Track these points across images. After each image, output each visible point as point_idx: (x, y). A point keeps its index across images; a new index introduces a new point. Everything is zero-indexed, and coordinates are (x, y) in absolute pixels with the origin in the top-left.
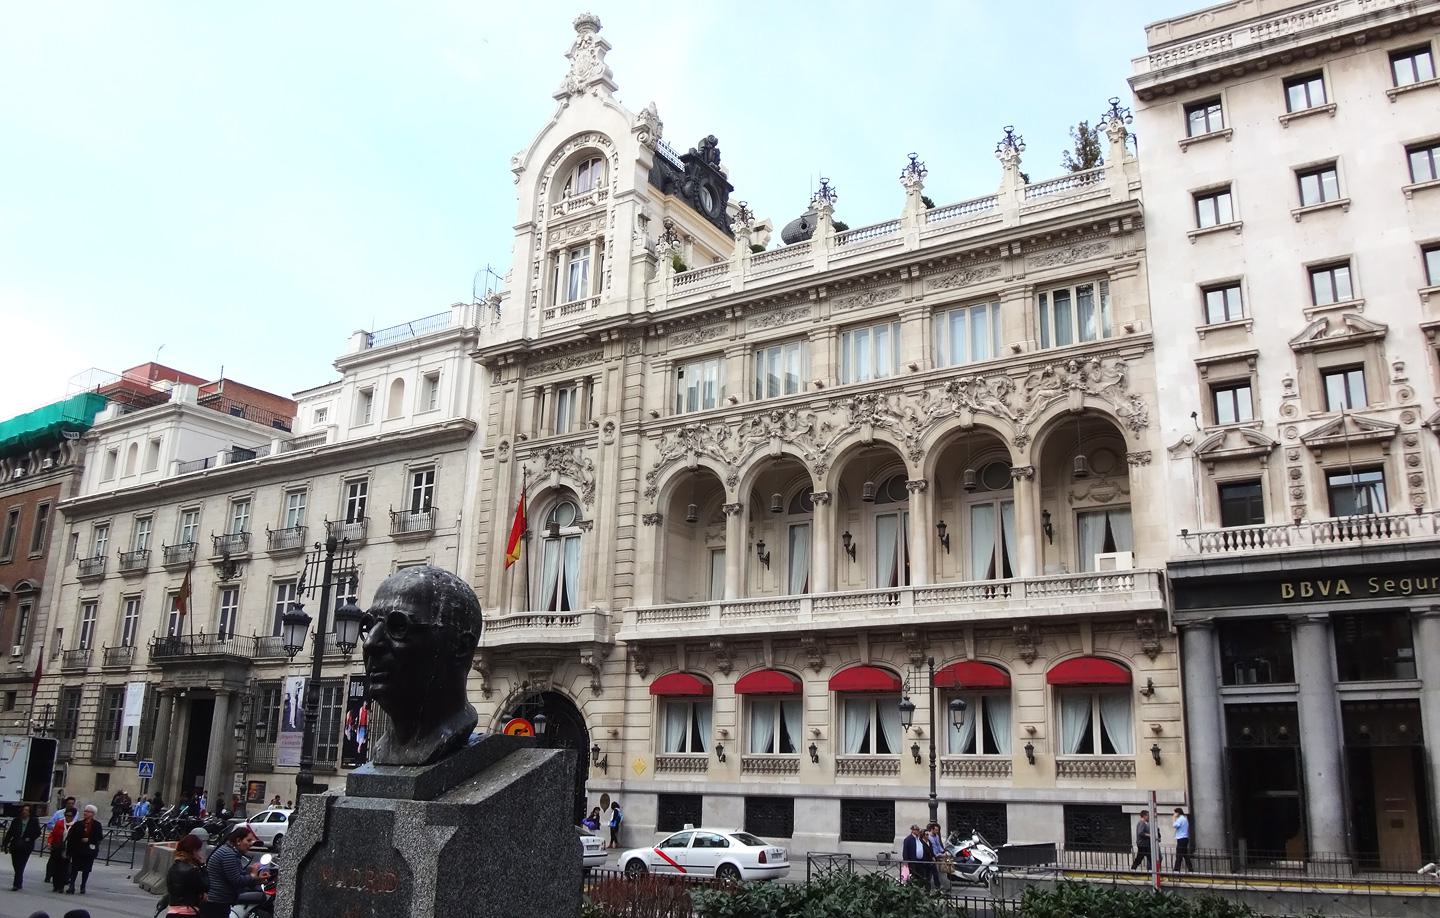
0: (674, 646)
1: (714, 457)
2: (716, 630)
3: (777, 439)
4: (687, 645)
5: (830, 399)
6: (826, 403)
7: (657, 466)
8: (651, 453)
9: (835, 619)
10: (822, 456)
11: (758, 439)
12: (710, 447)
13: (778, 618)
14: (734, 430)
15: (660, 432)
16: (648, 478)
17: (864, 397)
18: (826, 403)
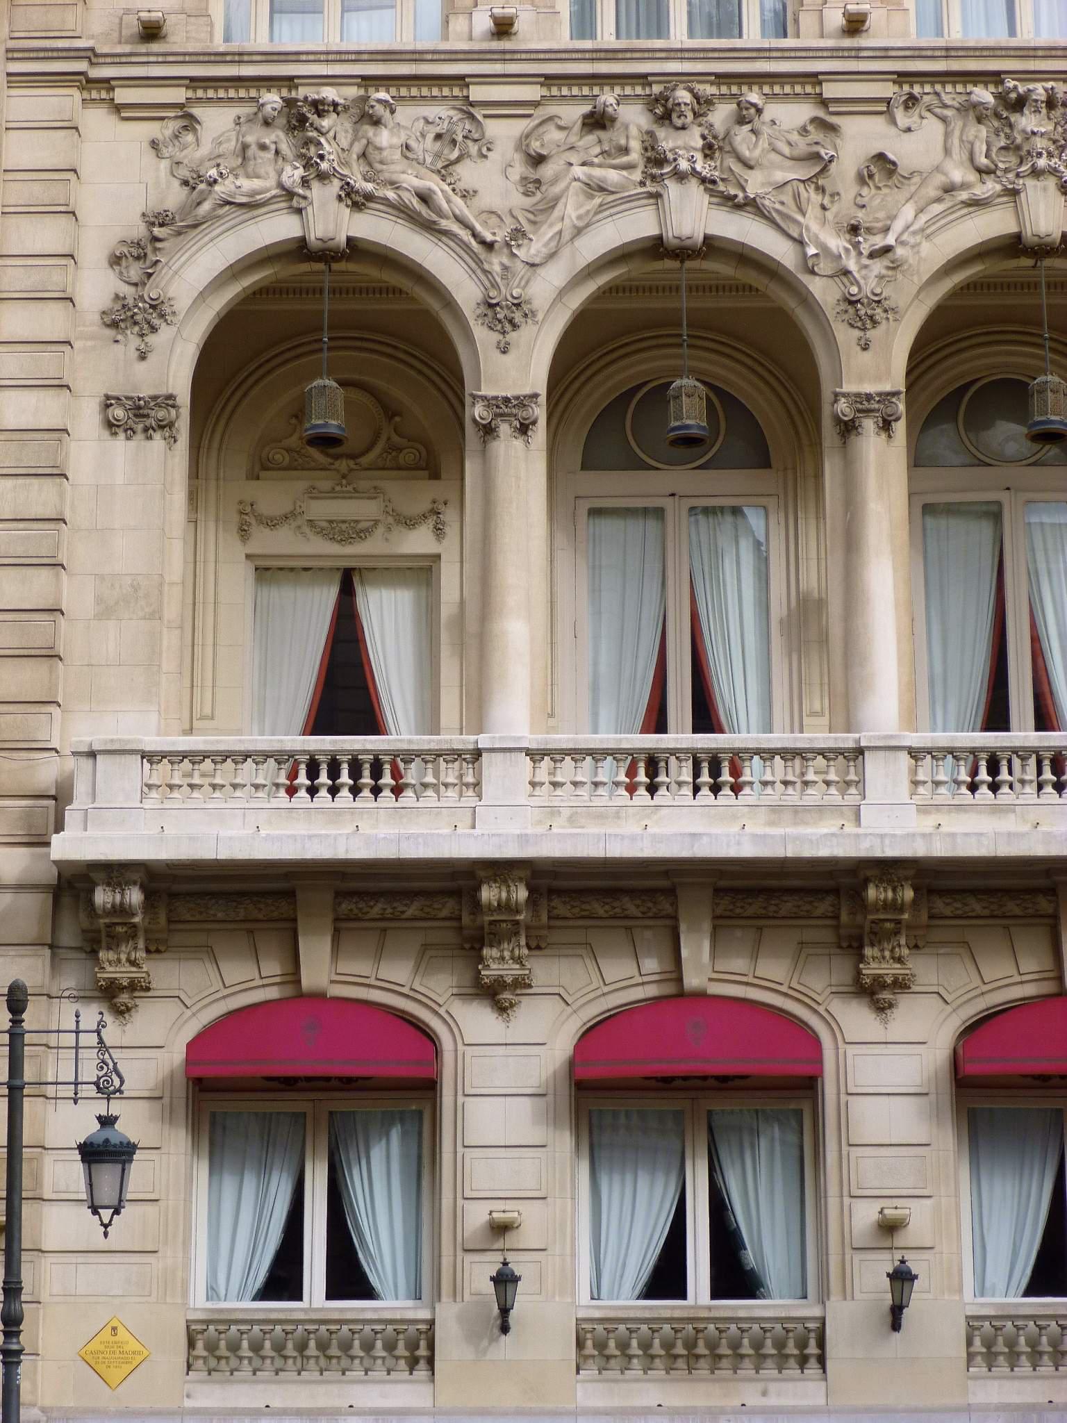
0: (290, 895)
1: (422, 215)
2: (523, 839)
3: (694, 187)
4: (340, 895)
5: (902, 77)
6: (886, 89)
7: (160, 219)
8: (121, 172)
9: (1009, 824)
10: (878, 266)
11: (613, 176)
12: (412, 179)
13: (776, 809)
14: (503, 132)
15: (178, 95)
16: (116, 260)
17: (1039, 90)
18: (886, 89)
